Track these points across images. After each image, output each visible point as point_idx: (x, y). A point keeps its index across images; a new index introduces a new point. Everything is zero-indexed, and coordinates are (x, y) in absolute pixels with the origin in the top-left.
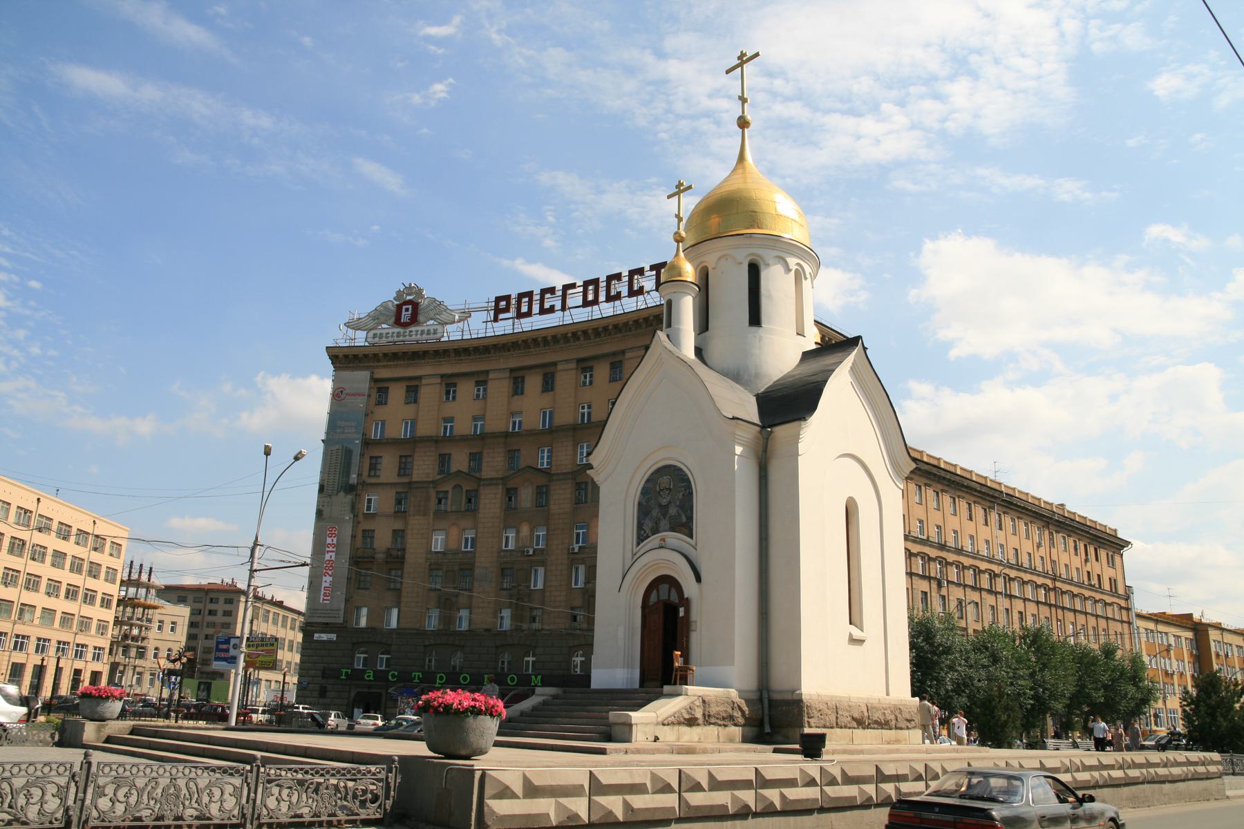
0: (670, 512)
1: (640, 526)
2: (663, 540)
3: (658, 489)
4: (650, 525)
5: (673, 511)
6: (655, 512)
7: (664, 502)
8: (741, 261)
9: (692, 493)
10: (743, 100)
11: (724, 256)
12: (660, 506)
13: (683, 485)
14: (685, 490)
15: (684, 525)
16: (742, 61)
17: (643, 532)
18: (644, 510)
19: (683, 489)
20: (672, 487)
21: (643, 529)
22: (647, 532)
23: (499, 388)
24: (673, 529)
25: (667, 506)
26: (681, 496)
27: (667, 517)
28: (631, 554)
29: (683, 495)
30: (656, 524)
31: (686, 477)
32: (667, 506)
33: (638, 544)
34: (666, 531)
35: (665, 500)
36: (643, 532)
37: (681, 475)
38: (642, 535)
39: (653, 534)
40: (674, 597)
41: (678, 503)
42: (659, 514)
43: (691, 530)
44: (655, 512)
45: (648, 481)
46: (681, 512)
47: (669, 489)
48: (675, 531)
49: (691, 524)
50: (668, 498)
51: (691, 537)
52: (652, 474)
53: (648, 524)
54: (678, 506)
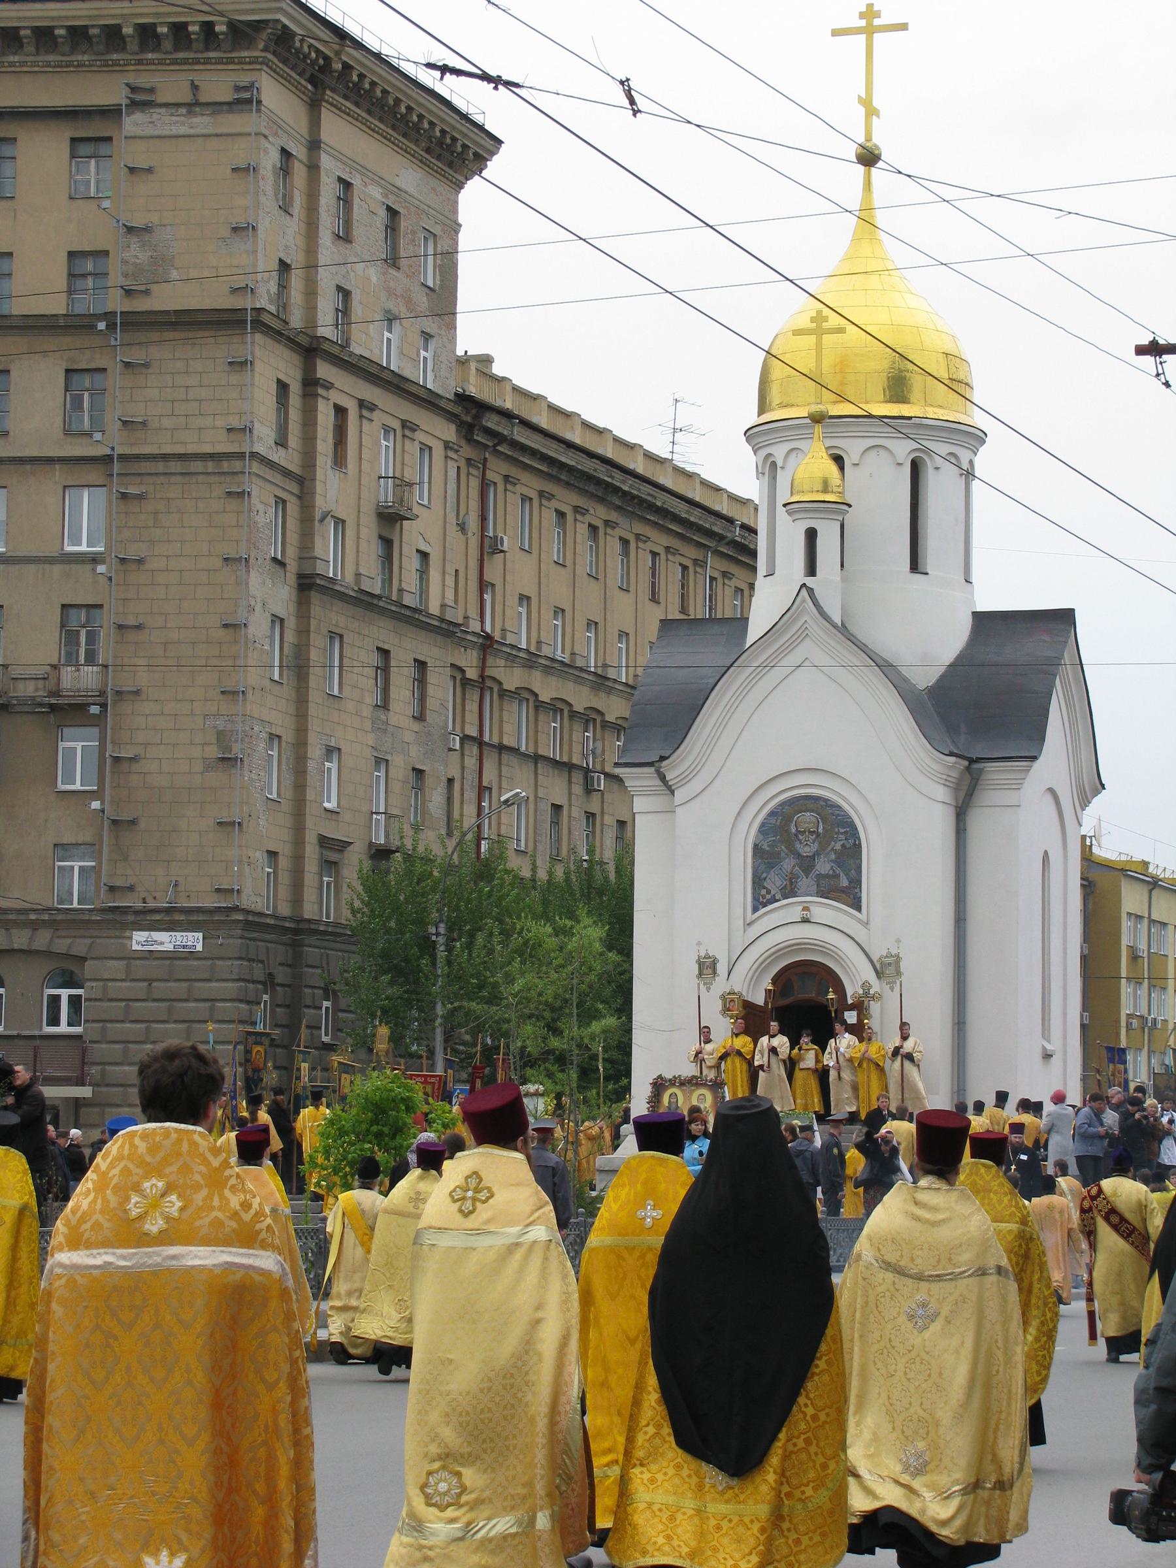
1: (758, 882)
2: (806, 909)
3: (793, 830)
4: (779, 883)
5: (823, 866)
7: (806, 851)
10: (871, 112)
12: (799, 856)
15: (843, 890)
17: (764, 892)
20: (820, 830)
21: (765, 888)
22: (773, 893)
27: (812, 875)
28: (741, 922)
29: (843, 846)
30: (791, 883)
35: (807, 849)
37: (839, 815)
38: (764, 897)
39: (785, 897)
41: (833, 857)
42: (797, 868)
43: (859, 899)
44: (789, 864)
46: (838, 870)
47: (818, 835)
51: (859, 909)
53: (774, 882)
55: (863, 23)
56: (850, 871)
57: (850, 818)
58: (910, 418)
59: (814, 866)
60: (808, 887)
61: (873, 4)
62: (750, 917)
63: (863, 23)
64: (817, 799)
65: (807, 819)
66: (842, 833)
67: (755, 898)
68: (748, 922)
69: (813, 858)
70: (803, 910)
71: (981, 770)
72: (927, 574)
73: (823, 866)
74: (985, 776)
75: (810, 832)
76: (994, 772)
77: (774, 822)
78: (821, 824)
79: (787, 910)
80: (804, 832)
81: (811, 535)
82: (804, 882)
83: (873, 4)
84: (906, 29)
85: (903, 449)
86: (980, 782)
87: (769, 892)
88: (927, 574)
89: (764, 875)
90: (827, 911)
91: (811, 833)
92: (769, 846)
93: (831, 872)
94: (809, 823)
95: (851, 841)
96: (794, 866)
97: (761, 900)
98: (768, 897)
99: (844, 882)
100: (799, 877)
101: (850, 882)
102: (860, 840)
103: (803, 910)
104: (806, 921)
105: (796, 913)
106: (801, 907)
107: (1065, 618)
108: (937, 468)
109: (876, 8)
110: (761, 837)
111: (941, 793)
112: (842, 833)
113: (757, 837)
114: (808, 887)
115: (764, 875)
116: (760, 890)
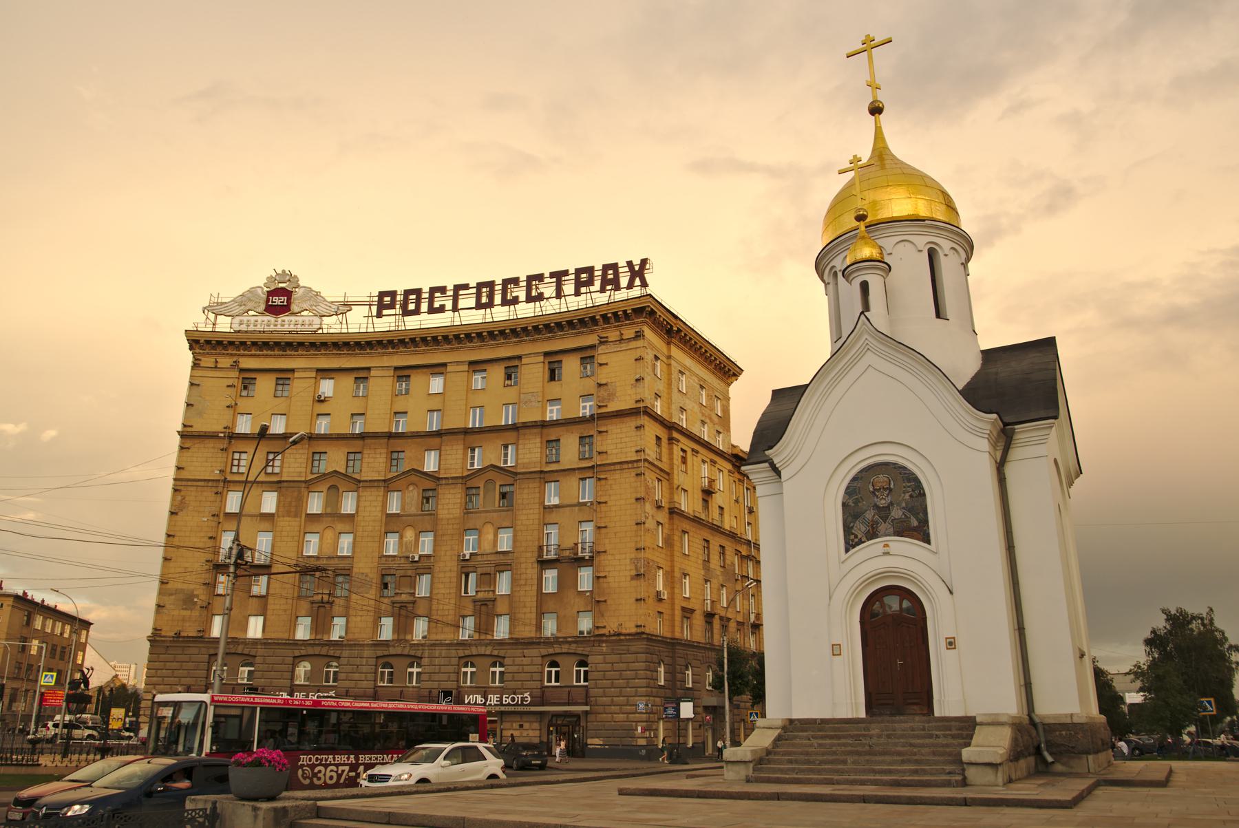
0: (893, 514)
1: (848, 530)
3: (871, 489)
4: (863, 529)
5: (896, 513)
6: (869, 515)
7: (882, 503)
8: (920, 249)
9: (924, 495)
12: (876, 507)
13: (908, 484)
14: (913, 490)
15: (915, 529)
17: (852, 537)
18: (851, 513)
20: (892, 486)
21: (853, 534)
22: (859, 537)
23: (533, 372)
24: (899, 533)
25: (888, 508)
26: (907, 496)
27: (889, 520)
29: (911, 496)
30: (873, 528)
31: (914, 476)
32: (888, 508)
33: (847, 551)
34: (889, 535)
35: (883, 502)
36: (852, 537)
37: (905, 474)
38: (853, 540)
41: (904, 505)
42: (876, 516)
44: (869, 515)
45: (854, 479)
47: (890, 490)
48: (902, 536)
50: (889, 499)
51: (929, 542)
53: (860, 529)
54: (904, 508)
56: (918, 514)
57: (914, 474)
60: (886, 529)
62: (844, 556)
65: (881, 479)
66: (909, 487)
67: (846, 542)
69: (888, 507)
70: (884, 547)
73: (896, 513)
74: (1016, 437)
75: (884, 488)
77: (855, 484)
78: (892, 482)
79: (872, 548)
80: (880, 489)
82: (883, 527)
84: (891, 41)
85: (922, 241)
87: (856, 536)
89: (852, 525)
92: (853, 503)
93: (903, 517)
94: (883, 482)
96: (874, 515)
97: (850, 544)
98: (856, 540)
99: (915, 523)
100: (878, 523)
101: (919, 523)
102: (923, 489)
103: (884, 547)
107: (1049, 344)
108: (946, 255)
110: (847, 497)
111: (984, 445)
112: (909, 487)
113: (844, 498)
114: (886, 529)
115: (852, 525)
116: (849, 536)
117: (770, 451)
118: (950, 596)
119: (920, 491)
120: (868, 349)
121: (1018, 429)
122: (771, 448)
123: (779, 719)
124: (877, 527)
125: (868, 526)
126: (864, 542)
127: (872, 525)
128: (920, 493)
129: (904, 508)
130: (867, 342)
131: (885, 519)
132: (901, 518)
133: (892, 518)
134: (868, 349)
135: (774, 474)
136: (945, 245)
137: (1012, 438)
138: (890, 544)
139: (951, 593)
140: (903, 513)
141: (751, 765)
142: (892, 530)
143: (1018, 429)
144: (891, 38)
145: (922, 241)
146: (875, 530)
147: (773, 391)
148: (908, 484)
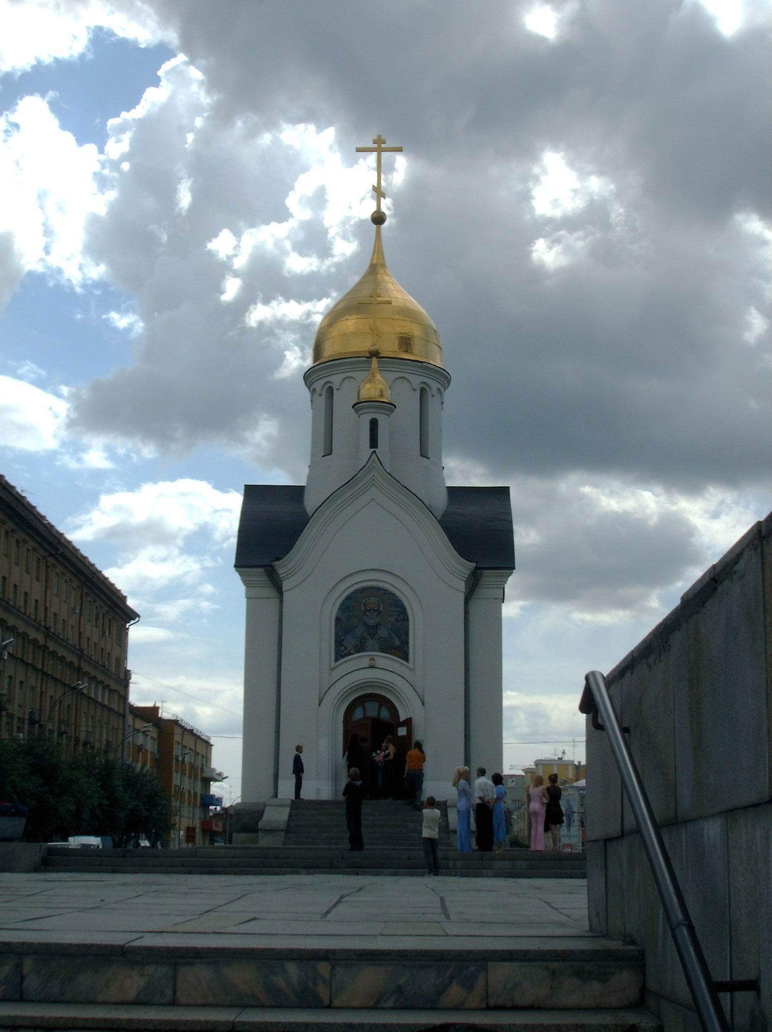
1: (339, 642)
4: (353, 643)
5: (383, 632)
7: (372, 622)
8: (415, 388)
9: (407, 620)
11: (402, 377)
13: (395, 609)
14: (398, 615)
16: (379, 146)
17: (342, 648)
19: (396, 614)
20: (381, 609)
21: (343, 646)
25: (376, 627)
26: (393, 620)
29: (397, 620)
32: (376, 627)
33: (337, 660)
34: (375, 651)
35: (372, 621)
38: (342, 652)
39: (359, 652)
40: (385, 714)
41: (390, 626)
42: (365, 633)
44: (360, 631)
45: (349, 598)
46: (393, 635)
47: (380, 612)
49: (406, 648)
50: (378, 619)
52: (355, 592)
53: (350, 642)
54: (389, 629)
55: (376, 146)
57: (400, 601)
58: (422, 362)
59: (377, 632)
61: (381, 136)
62: (333, 664)
63: (376, 146)
64: (379, 589)
66: (396, 611)
68: (333, 667)
69: (377, 625)
70: (371, 660)
71: (481, 574)
72: (429, 458)
75: (375, 611)
76: (488, 577)
78: (381, 605)
79: (359, 660)
81: (374, 424)
82: (370, 643)
83: (381, 136)
85: (417, 380)
86: (480, 583)
87: (346, 649)
88: (429, 458)
89: (343, 638)
90: (385, 660)
91: (375, 611)
95: (402, 616)
96: (363, 632)
98: (346, 651)
99: (398, 643)
102: (408, 616)
104: (372, 667)
105: (365, 662)
106: (369, 659)
107: (504, 492)
108: (433, 396)
109: (383, 138)
113: (338, 613)
115: (343, 638)
117: (277, 563)
118: (422, 707)
119: (404, 616)
120: (373, 484)
121: (487, 573)
122: (278, 559)
123: (288, 799)
124: (365, 643)
125: (358, 641)
126: (353, 654)
127: (361, 640)
128: (404, 618)
129: (389, 629)
130: (374, 478)
131: (372, 636)
132: (386, 637)
133: (379, 636)
134: (373, 484)
135: (268, 579)
136: (434, 385)
137: (479, 581)
138: (376, 658)
139: (423, 704)
140: (389, 633)
141: (283, 833)
142: (377, 646)
143: (487, 573)
144: (402, 148)
145: (417, 380)
146: (363, 645)
147: (246, 486)
148: (395, 609)
